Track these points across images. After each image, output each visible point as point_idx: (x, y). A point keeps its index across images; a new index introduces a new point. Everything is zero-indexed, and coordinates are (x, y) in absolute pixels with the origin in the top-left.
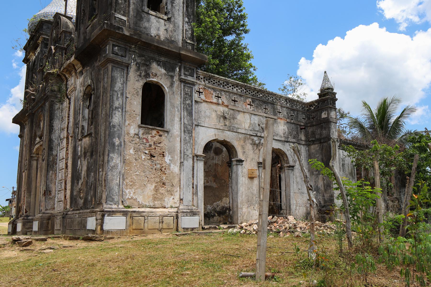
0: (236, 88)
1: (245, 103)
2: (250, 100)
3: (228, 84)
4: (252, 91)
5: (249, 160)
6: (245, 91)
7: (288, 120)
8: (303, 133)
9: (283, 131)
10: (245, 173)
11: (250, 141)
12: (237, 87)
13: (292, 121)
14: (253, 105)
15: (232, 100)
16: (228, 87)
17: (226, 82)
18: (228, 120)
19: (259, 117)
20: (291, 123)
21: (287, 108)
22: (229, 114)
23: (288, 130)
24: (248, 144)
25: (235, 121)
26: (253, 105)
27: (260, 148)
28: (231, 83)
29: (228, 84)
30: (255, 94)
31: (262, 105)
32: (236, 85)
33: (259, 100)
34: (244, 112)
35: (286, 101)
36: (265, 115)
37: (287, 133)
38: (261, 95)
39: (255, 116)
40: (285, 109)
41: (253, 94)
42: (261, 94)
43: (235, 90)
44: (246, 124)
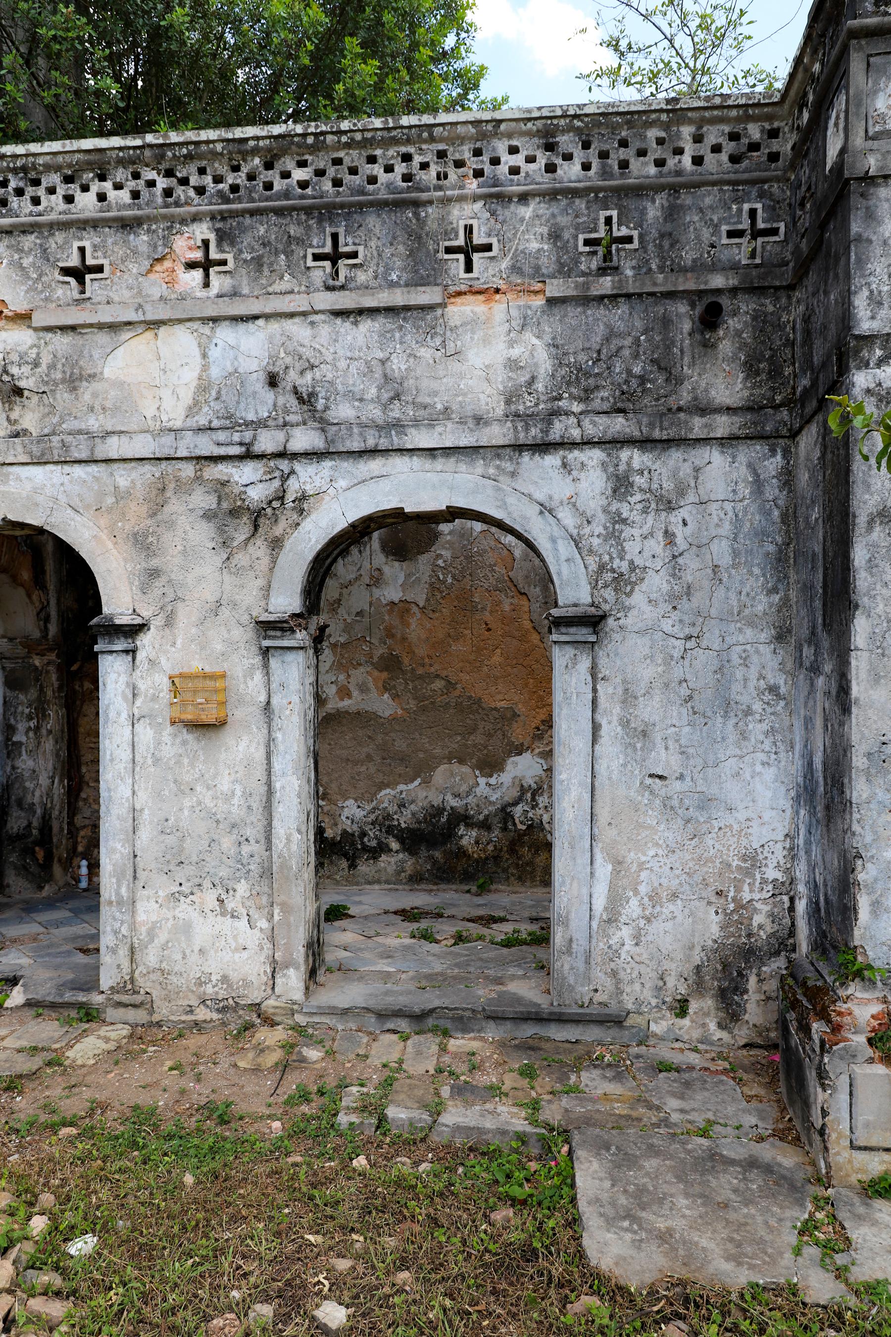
0: (95, 187)
1: (167, 264)
2: (203, 231)
3: (36, 183)
4: (222, 168)
5: (186, 616)
6: (162, 183)
7: (555, 289)
8: (726, 347)
9: (500, 377)
10: (155, 698)
11: (203, 500)
12: (102, 178)
13: (606, 285)
14: (224, 263)
15: (67, 271)
16: (36, 201)
17: (15, 171)
18: (35, 399)
19: (274, 326)
20: (585, 300)
21: (552, 195)
22: (45, 360)
23: (559, 362)
24: (183, 522)
25: (87, 397)
26: (224, 263)
27: (278, 531)
28: (48, 168)
29: (36, 183)
30: (251, 177)
31: (300, 241)
32: (89, 166)
33: (279, 212)
34: (155, 325)
35: (550, 147)
36: (326, 300)
37: (540, 386)
38: (299, 174)
39: (242, 327)
40: (527, 212)
41: (235, 188)
42: (302, 164)
43: (87, 203)
44: (166, 394)
